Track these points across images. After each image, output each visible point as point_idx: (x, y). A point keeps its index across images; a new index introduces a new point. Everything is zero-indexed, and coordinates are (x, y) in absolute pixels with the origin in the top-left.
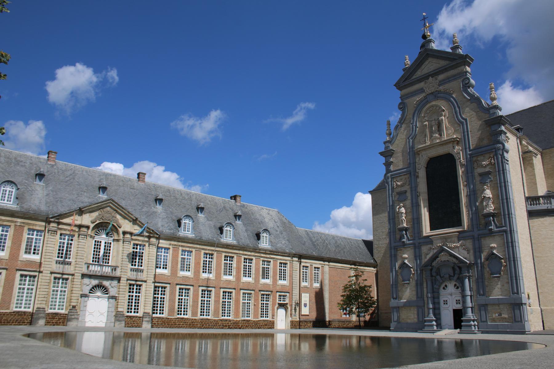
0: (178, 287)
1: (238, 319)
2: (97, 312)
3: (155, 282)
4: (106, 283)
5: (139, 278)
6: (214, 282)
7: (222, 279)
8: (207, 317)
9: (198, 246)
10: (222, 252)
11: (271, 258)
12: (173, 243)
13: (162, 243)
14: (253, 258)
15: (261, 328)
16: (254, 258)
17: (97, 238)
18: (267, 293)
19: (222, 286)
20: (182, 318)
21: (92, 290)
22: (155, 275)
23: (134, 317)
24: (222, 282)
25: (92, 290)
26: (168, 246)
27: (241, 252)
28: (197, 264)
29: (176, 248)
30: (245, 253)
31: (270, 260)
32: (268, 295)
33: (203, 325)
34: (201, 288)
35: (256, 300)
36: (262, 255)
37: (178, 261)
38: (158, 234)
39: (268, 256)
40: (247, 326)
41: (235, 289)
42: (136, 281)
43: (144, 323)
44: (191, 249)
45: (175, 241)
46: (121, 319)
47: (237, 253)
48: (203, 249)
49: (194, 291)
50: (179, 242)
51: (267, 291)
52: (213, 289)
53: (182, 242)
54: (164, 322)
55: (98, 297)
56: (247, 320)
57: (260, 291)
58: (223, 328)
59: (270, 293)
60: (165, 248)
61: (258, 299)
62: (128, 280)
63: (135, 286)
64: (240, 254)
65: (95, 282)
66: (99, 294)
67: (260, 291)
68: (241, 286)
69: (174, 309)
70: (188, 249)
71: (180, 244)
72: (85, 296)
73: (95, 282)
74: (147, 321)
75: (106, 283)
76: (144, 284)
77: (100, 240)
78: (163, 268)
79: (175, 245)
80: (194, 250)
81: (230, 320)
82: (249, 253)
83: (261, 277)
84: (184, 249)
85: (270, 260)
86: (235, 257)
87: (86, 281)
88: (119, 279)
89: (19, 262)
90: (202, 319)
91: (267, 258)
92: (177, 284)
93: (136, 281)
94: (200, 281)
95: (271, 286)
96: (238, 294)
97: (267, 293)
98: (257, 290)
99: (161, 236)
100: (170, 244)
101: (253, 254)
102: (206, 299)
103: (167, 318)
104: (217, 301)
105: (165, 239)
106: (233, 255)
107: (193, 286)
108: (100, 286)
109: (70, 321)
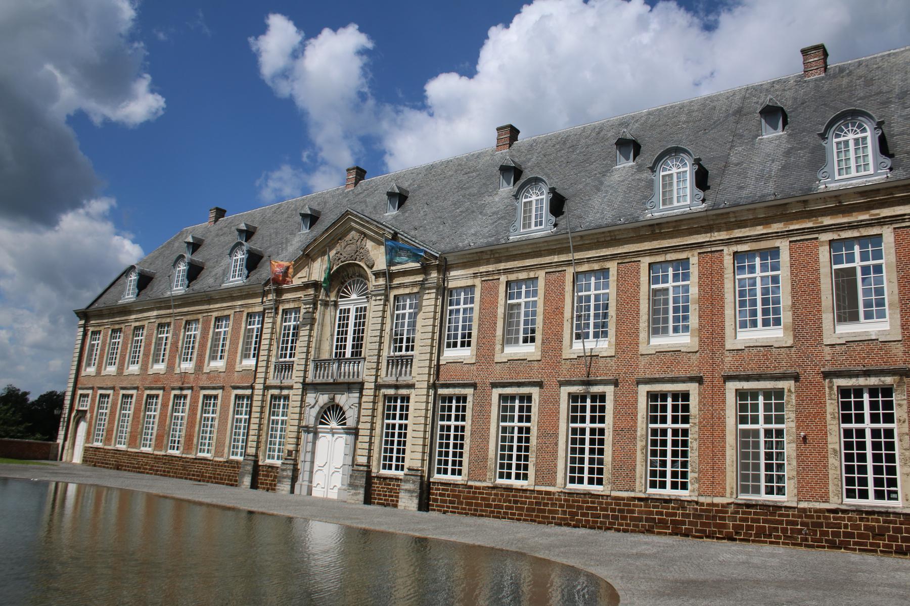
0: (496, 392)
1: (717, 500)
2: (330, 465)
3: (434, 386)
4: (342, 399)
5: (403, 379)
6: (612, 363)
7: (643, 349)
8: (596, 488)
9: (556, 258)
10: (639, 253)
11: (881, 222)
12: (483, 269)
13: (456, 278)
14: (777, 243)
15: (844, 546)
16: (784, 245)
17: (343, 304)
18: (873, 381)
19: (641, 375)
20: (509, 489)
21: (322, 418)
22: (438, 366)
23: (391, 479)
24: (643, 361)
25: (322, 418)
26: (469, 282)
27: (723, 235)
28: (554, 312)
29: (489, 279)
30: (738, 233)
31: (874, 231)
32: (888, 391)
33: (573, 515)
34: (565, 391)
35: (811, 418)
36: (827, 221)
37: (496, 317)
38: (436, 258)
39: (864, 216)
40: (761, 532)
41: (699, 380)
42: (397, 387)
43: (402, 495)
44: (532, 275)
45: (488, 263)
46: (358, 482)
47: (700, 245)
48: (569, 263)
49: (543, 401)
50: (499, 261)
51: (867, 374)
52: (609, 390)
53: (507, 260)
54: (458, 497)
55: (333, 432)
56: (765, 506)
57: (827, 375)
58: (650, 531)
59: (889, 380)
60: (465, 288)
61: (822, 415)
62: (378, 387)
63: (395, 403)
64: (711, 243)
65: (324, 399)
66: (334, 424)
67: (827, 375)
68: (728, 364)
69: (485, 458)
70: (523, 275)
71: (502, 266)
72: (307, 429)
73: (324, 399)
74: (409, 491)
75: (342, 399)
76: (412, 393)
77: (347, 307)
78: (463, 345)
79: (488, 273)
80: (541, 274)
81: (681, 503)
82: (760, 230)
83: (828, 318)
84: (512, 277)
85: (874, 231)
86: (694, 260)
87: (310, 398)
88: (360, 386)
89: (236, 374)
90: (748, 506)
91: (851, 226)
92: (494, 385)
93: (397, 387)
94: (565, 366)
95: (898, 350)
96: (714, 401)
97: (873, 381)
98: (811, 374)
99: (451, 259)
100: (475, 275)
101: (777, 227)
102: (588, 425)
103: (466, 486)
104: (625, 431)
105: (464, 265)
106: (682, 256)
107: (540, 384)
108: (333, 409)
109: (279, 482)
